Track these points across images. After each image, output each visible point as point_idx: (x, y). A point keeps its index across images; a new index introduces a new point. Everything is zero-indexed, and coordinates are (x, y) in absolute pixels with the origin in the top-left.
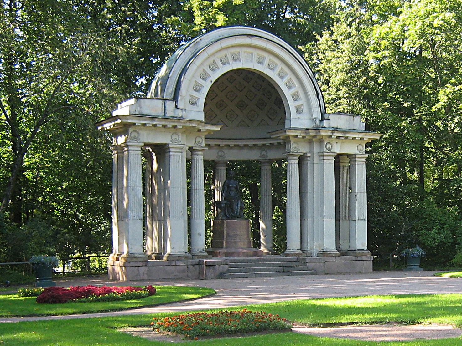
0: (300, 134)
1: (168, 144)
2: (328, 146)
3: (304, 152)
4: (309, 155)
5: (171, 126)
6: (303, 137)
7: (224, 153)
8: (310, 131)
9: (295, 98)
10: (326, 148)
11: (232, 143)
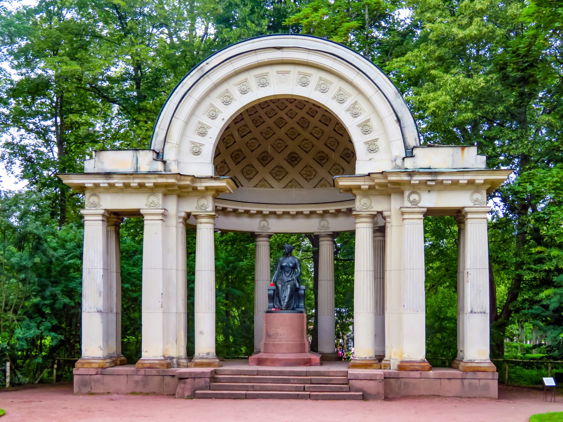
0: (365, 184)
1: (139, 210)
2: (414, 197)
3: (380, 210)
4: (385, 214)
5: (136, 185)
6: (371, 188)
7: (328, 222)
8: (373, 176)
9: (365, 128)
10: (409, 200)
11: (332, 208)
